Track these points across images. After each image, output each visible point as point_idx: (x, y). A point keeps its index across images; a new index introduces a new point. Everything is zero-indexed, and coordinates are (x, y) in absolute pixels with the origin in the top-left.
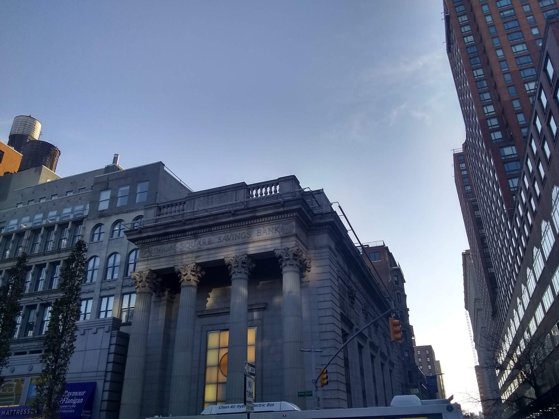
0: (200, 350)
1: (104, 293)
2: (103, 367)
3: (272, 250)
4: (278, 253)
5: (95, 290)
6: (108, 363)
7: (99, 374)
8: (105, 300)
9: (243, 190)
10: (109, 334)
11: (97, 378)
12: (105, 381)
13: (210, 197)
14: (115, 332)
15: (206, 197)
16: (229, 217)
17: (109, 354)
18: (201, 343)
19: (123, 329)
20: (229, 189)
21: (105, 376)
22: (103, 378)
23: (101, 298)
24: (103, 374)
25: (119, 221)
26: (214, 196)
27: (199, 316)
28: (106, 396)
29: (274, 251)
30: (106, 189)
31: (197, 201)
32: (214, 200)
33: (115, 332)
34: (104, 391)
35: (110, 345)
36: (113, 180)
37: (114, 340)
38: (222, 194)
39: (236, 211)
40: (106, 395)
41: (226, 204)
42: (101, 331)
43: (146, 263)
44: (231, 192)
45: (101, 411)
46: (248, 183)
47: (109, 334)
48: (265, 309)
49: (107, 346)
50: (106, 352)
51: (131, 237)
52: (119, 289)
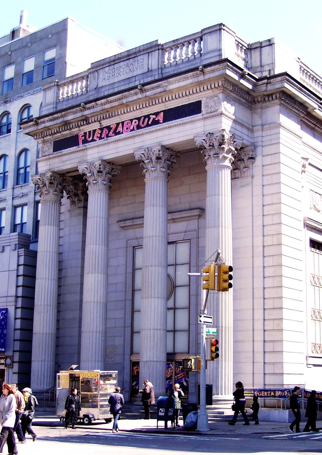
0: (126, 271)
1: (17, 202)
2: (12, 292)
3: (191, 137)
4: (199, 142)
5: (7, 198)
6: (17, 286)
7: (10, 299)
8: (19, 210)
9: (157, 52)
10: (16, 252)
11: (8, 304)
12: (16, 308)
13: (116, 66)
14: (22, 251)
15: (111, 67)
16: (136, 94)
17: (18, 276)
18: (126, 261)
19: (32, 247)
20: (140, 51)
21: (16, 302)
22: (14, 303)
23: (15, 208)
24: (13, 299)
25: (27, 107)
26: (122, 64)
27: (123, 227)
28: (18, 324)
29: (194, 139)
30: (10, 64)
31: (101, 72)
32: (122, 70)
33: (22, 251)
34: (16, 319)
35: (18, 265)
36: (15, 50)
37: (22, 261)
38: (131, 60)
39: (144, 85)
40: (18, 322)
41: (135, 74)
42: (7, 249)
43: (48, 162)
44: (142, 57)
45: (15, 340)
46: (161, 42)
47: (16, 252)
48: (200, 216)
49: (15, 267)
50: (14, 274)
51: (27, 131)
52: (32, 195)
